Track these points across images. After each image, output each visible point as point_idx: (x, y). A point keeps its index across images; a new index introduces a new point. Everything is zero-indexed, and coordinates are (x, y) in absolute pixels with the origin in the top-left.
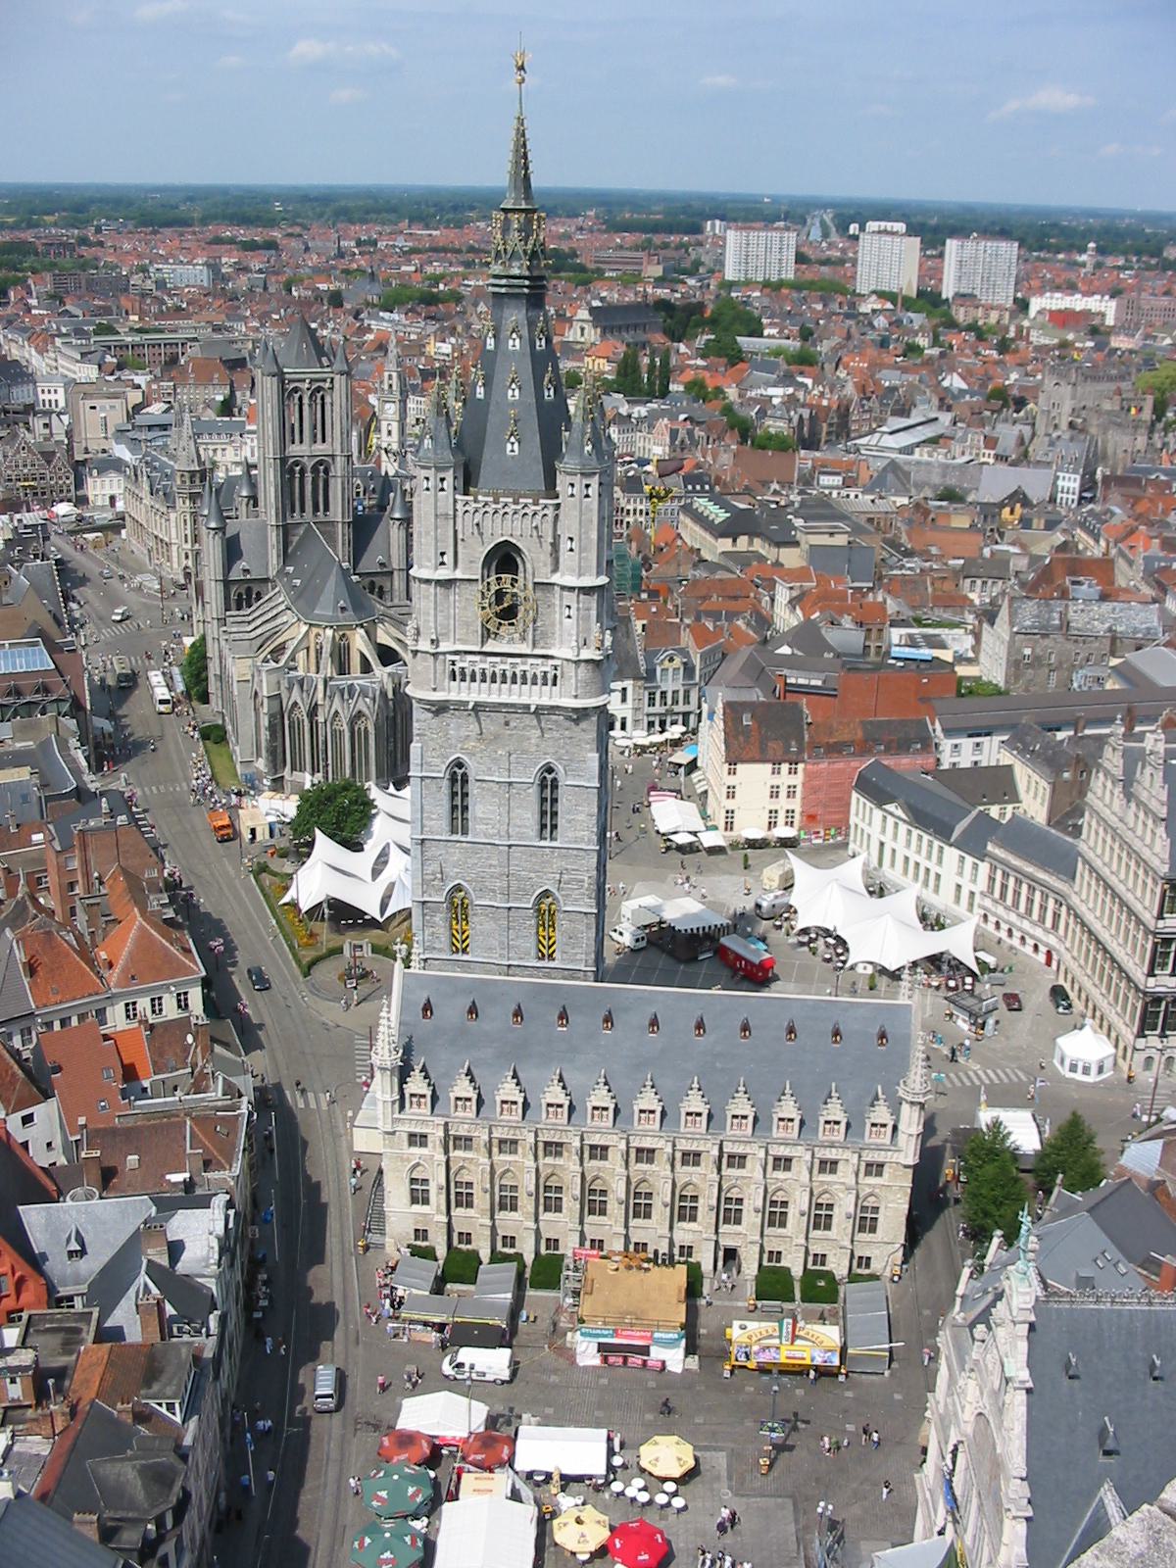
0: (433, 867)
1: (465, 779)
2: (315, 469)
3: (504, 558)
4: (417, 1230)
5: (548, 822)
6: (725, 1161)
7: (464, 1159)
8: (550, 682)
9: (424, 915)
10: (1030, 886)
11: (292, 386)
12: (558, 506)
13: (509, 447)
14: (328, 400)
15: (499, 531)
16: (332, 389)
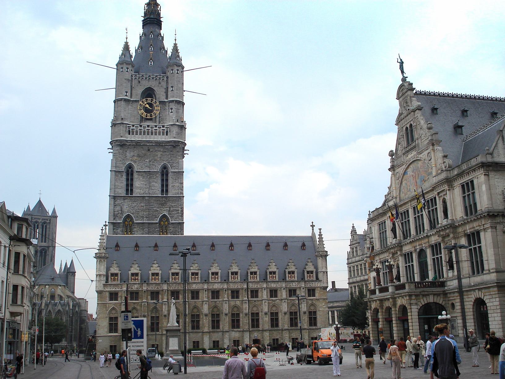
0: (118, 208)
1: (132, 171)
2: (41, 252)
3: (149, 93)
4: (111, 346)
5: (165, 188)
6: (249, 293)
7: (134, 303)
8: (165, 133)
9: (114, 229)
10: (331, 311)
11: (35, 220)
12: (167, 77)
14: (48, 227)
15: (146, 84)
16: (50, 223)
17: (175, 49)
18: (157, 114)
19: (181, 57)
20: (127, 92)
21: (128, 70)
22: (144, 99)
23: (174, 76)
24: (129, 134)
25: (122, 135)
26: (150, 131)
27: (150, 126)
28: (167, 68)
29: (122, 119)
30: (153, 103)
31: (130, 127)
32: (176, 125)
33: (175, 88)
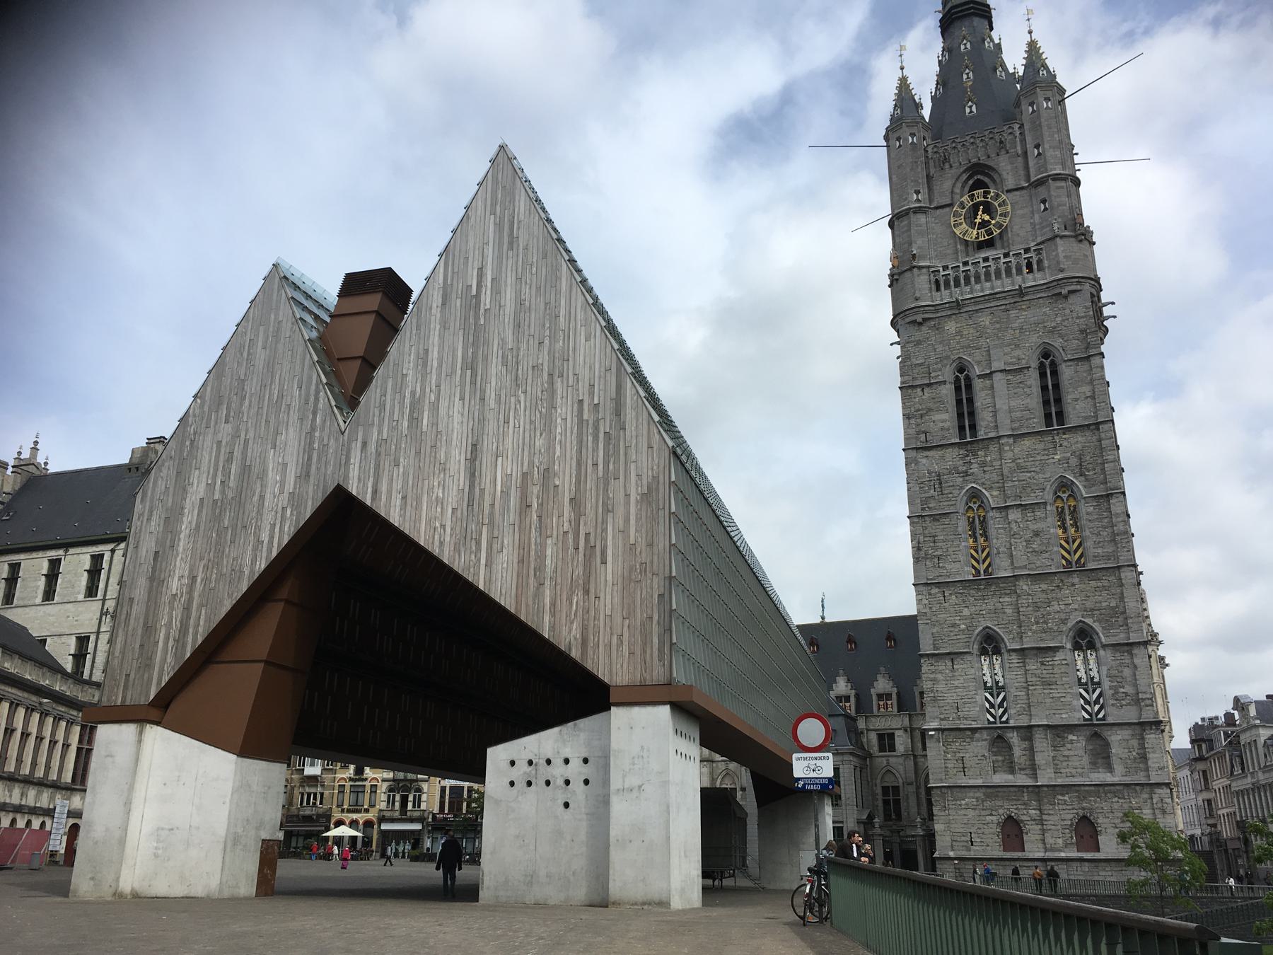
12: (1022, 126)
13: (968, 110)
17: (1033, 51)
18: (1005, 224)
19: (1052, 71)
20: (917, 192)
21: (915, 139)
22: (964, 198)
23: (1039, 117)
24: (938, 289)
25: (918, 295)
26: (993, 269)
27: (991, 258)
28: (1018, 104)
29: (914, 256)
30: (989, 200)
31: (938, 271)
32: (1062, 237)
33: (1047, 146)
